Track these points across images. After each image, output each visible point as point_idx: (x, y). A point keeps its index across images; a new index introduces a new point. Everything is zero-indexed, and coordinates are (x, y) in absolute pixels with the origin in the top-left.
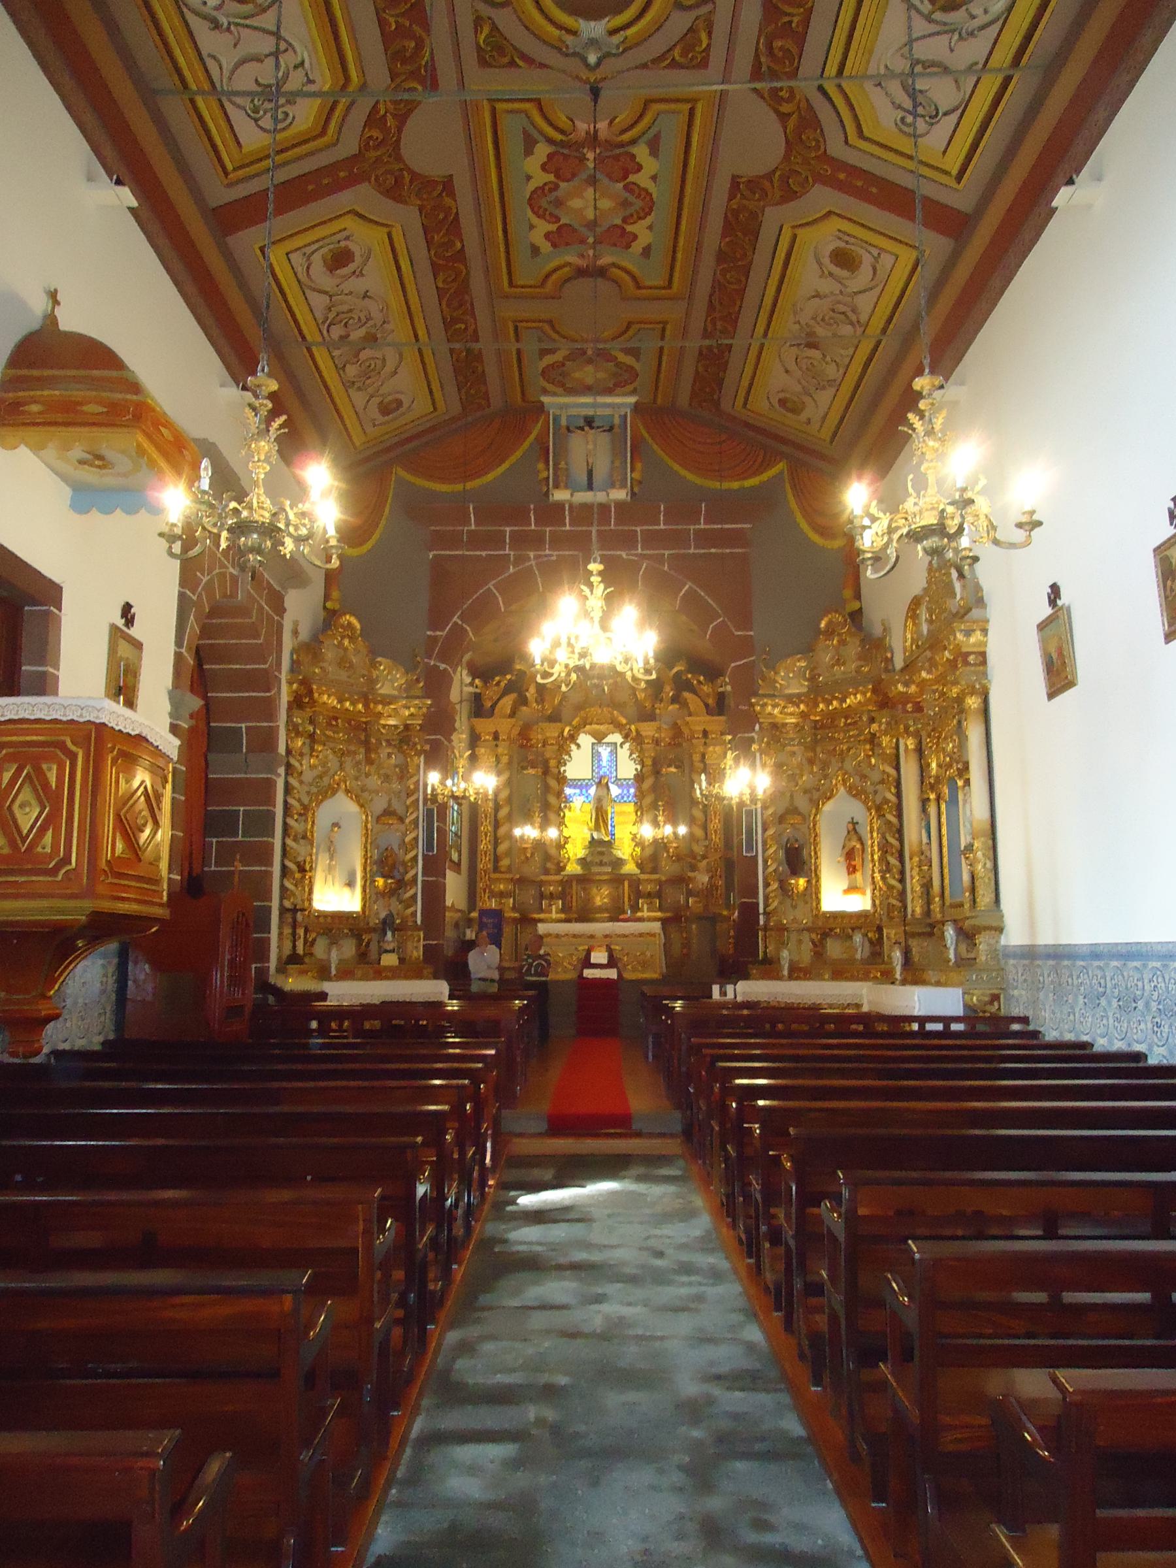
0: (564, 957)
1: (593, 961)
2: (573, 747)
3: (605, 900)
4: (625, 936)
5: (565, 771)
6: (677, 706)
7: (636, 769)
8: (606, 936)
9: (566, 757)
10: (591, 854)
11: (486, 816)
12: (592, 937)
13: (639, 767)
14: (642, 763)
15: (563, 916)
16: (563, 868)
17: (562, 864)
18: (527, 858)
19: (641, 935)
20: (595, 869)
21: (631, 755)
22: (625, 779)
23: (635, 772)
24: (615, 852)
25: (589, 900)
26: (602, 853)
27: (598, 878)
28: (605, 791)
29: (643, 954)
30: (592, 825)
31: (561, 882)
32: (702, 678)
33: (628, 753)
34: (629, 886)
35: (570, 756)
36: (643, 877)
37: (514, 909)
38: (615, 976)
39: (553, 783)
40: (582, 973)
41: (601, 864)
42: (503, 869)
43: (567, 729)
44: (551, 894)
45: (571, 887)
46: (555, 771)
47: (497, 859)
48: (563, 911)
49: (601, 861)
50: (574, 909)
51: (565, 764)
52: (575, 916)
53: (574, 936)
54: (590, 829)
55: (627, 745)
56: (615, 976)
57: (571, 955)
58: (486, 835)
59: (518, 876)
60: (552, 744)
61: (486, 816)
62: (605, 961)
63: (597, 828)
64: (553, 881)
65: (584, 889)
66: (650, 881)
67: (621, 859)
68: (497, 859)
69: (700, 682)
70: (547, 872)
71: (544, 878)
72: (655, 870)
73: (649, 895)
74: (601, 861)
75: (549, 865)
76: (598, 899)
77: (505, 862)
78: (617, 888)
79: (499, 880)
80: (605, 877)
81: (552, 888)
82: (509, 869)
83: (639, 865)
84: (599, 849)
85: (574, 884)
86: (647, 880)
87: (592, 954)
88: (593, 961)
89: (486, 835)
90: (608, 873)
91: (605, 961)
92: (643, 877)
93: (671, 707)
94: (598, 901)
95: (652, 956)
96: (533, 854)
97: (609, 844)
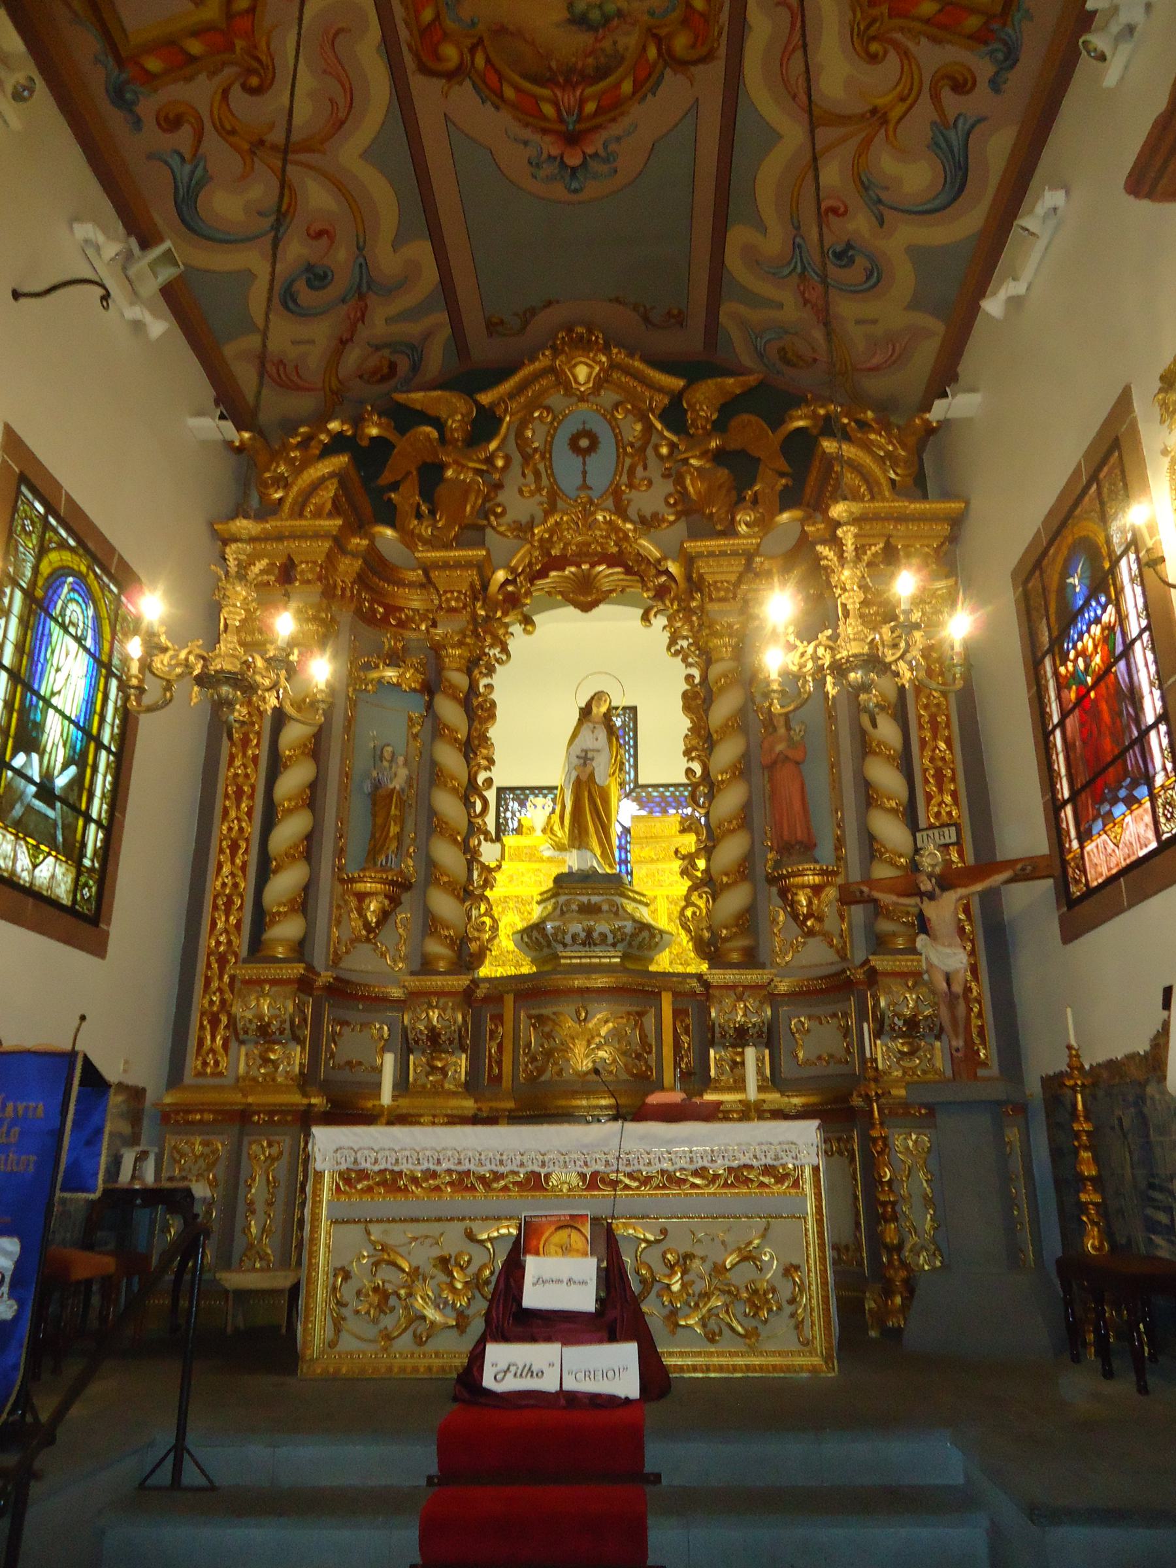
0: (415, 1273)
1: (532, 1298)
2: (516, 629)
3: (601, 1054)
4: (671, 1180)
5: (489, 687)
6: (797, 513)
7: (689, 678)
8: (593, 1181)
9: (495, 652)
10: (562, 911)
11: (239, 793)
12: (535, 1182)
13: (696, 672)
14: (707, 658)
15: (468, 1105)
16: (479, 958)
17: (474, 947)
18: (367, 925)
19: (739, 1176)
20: (571, 957)
21: (673, 642)
22: (655, 786)
23: (686, 687)
24: (630, 907)
25: (553, 1053)
26: (590, 910)
27: (578, 982)
28: (602, 734)
29: (749, 1257)
30: (562, 834)
31: (467, 996)
32: (870, 414)
33: (665, 637)
34: (677, 1013)
35: (505, 650)
36: (718, 977)
37: (305, 1080)
38: (628, 1386)
39: (450, 712)
40: (477, 1358)
41: (589, 940)
42: (280, 952)
43: (501, 575)
44: (434, 1036)
45: (498, 1018)
46: (460, 680)
47: (261, 919)
48: (471, 1087)
49: (589, 932)
50: (507, 1082)
51: (491, 671)
52: (511, 1105)
53: (463, 1182)
54: (559, 847)
55: (660, 621)
56: (628, 1386)
57: (444, 1263)
58: (234, 847)
59: (325, 977)
60: (453, 610)
61: (239, 793)
62: (584, 1300)
63: (578, 838)
64: (440, 994)
65: (541, 1019)
66: (739, 991)
67: (644, 926)
68: (261, 919)
69: (863, 425)
70: (426, 966)
71: (413, 983)
72: (751, 959)
73: (741, 1037)
74: (589, 932)
75: (435, 947)
76: (579, 1048)
77: (287, 930)
78: (640, 1014)
79: (255, 983)
80: (600, 981)
81: (434, 1015)
82: (301, 949)
83: (708, 948)
84: (584, 899)
85: (509, 1000)
86: (731, 987)
87: (532, 1264)
88: (532, 1298)
89: (234, 847)
90: (609, 969)
91: (584, 1300)
92: (718, 977)
93: (785, 516)
94: (581, 1060)
95: (789, 1270)
96: (385, 916)
97: (616, 884)
